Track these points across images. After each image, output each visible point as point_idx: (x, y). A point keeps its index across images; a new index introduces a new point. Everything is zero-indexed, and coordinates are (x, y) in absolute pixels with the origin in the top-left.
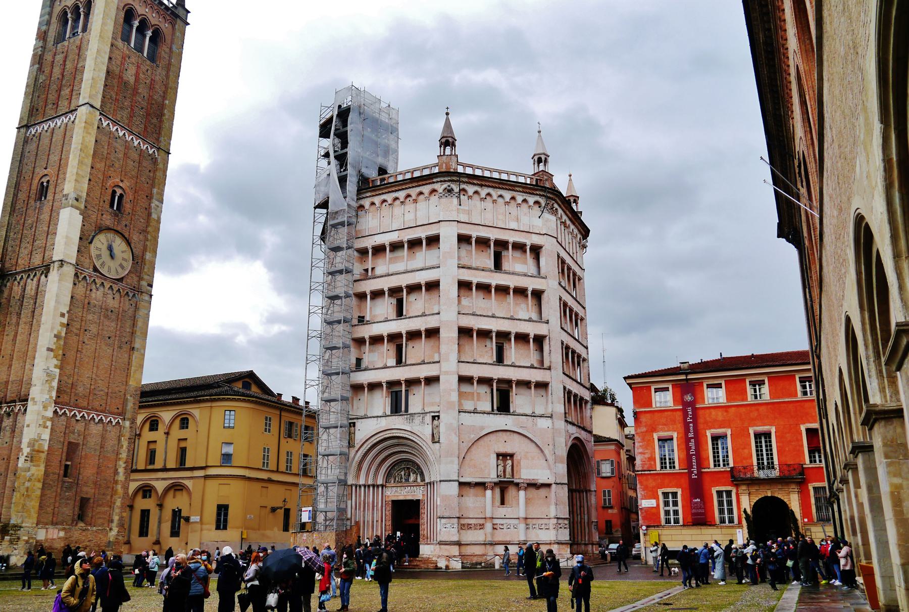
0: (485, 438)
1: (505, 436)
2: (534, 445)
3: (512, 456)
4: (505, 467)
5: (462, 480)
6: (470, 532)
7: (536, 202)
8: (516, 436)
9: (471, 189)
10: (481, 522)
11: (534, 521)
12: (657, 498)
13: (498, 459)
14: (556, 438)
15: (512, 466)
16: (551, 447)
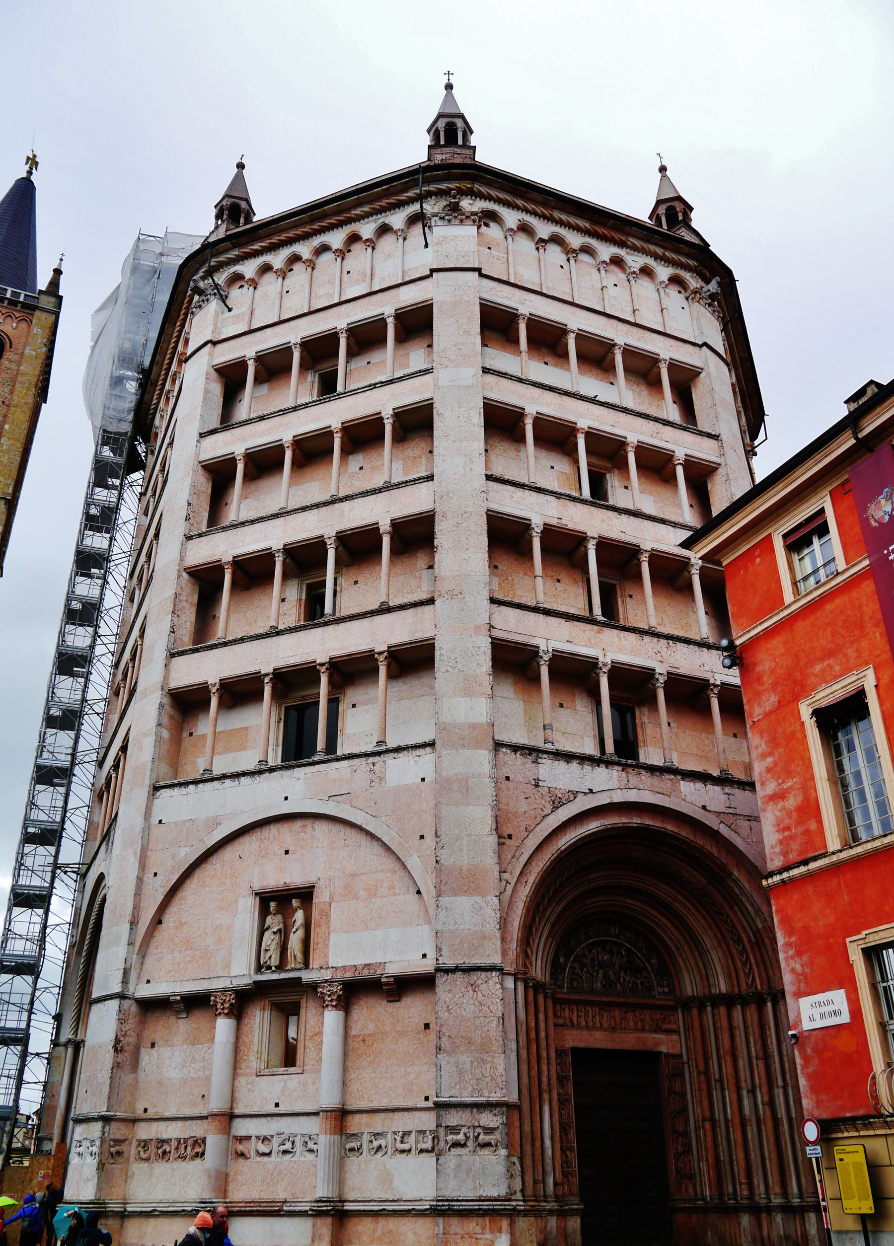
0: (229, 854)
1: (284, 834)
2: (377, 848)
3: (306, 895)
4: (284, 934)
5: (144, 991)
6: (161, 1168)
7: (413, 220)
8: (322, 829)
9: (249, 269)
10: (197, 1130)
11: (378, 1123)
12: (848, 982)
13: (264, 912)
14: (444, 810)
15: (307, 926)
16: (430, 840)
